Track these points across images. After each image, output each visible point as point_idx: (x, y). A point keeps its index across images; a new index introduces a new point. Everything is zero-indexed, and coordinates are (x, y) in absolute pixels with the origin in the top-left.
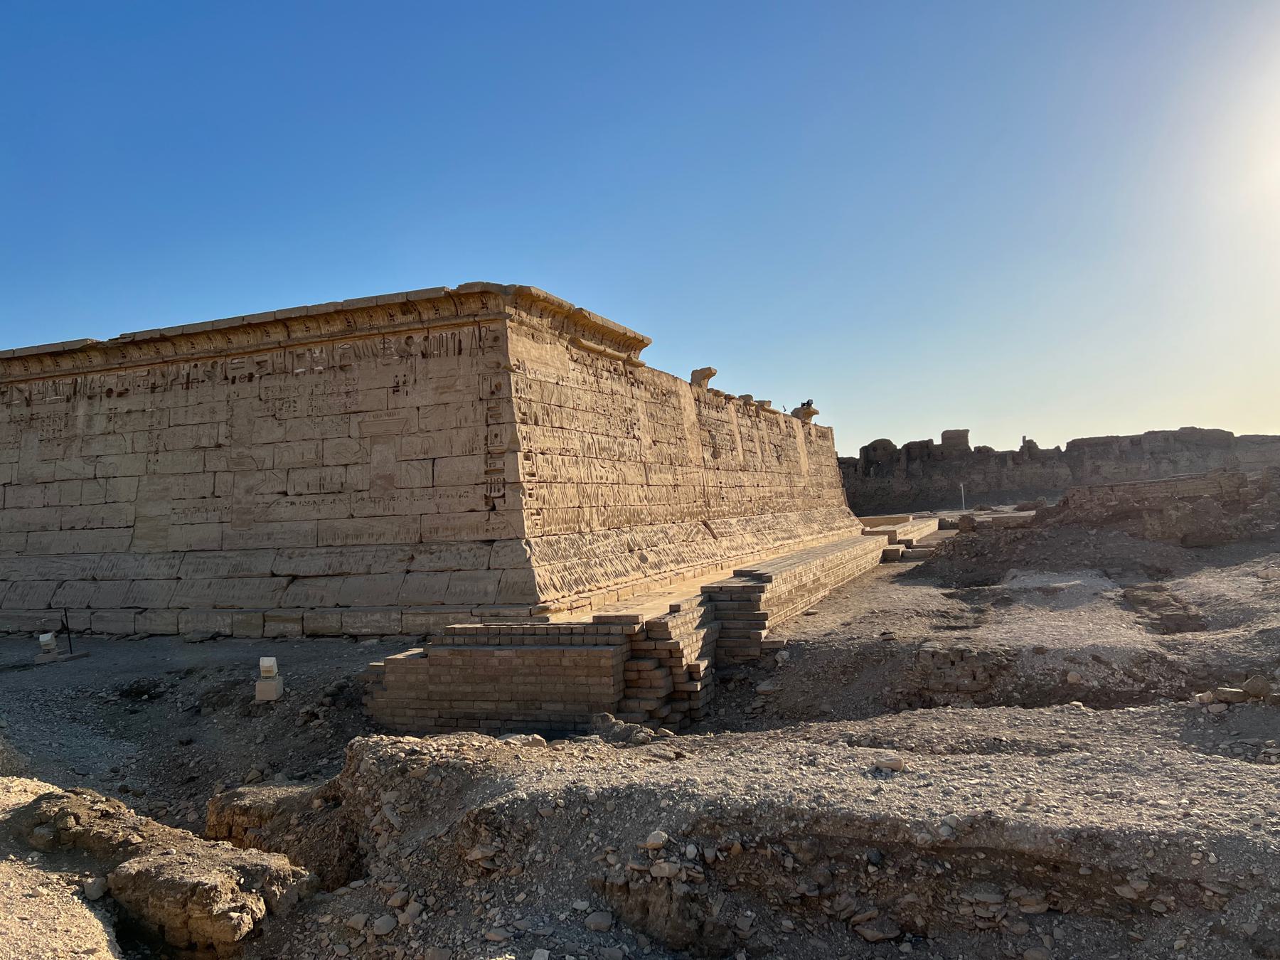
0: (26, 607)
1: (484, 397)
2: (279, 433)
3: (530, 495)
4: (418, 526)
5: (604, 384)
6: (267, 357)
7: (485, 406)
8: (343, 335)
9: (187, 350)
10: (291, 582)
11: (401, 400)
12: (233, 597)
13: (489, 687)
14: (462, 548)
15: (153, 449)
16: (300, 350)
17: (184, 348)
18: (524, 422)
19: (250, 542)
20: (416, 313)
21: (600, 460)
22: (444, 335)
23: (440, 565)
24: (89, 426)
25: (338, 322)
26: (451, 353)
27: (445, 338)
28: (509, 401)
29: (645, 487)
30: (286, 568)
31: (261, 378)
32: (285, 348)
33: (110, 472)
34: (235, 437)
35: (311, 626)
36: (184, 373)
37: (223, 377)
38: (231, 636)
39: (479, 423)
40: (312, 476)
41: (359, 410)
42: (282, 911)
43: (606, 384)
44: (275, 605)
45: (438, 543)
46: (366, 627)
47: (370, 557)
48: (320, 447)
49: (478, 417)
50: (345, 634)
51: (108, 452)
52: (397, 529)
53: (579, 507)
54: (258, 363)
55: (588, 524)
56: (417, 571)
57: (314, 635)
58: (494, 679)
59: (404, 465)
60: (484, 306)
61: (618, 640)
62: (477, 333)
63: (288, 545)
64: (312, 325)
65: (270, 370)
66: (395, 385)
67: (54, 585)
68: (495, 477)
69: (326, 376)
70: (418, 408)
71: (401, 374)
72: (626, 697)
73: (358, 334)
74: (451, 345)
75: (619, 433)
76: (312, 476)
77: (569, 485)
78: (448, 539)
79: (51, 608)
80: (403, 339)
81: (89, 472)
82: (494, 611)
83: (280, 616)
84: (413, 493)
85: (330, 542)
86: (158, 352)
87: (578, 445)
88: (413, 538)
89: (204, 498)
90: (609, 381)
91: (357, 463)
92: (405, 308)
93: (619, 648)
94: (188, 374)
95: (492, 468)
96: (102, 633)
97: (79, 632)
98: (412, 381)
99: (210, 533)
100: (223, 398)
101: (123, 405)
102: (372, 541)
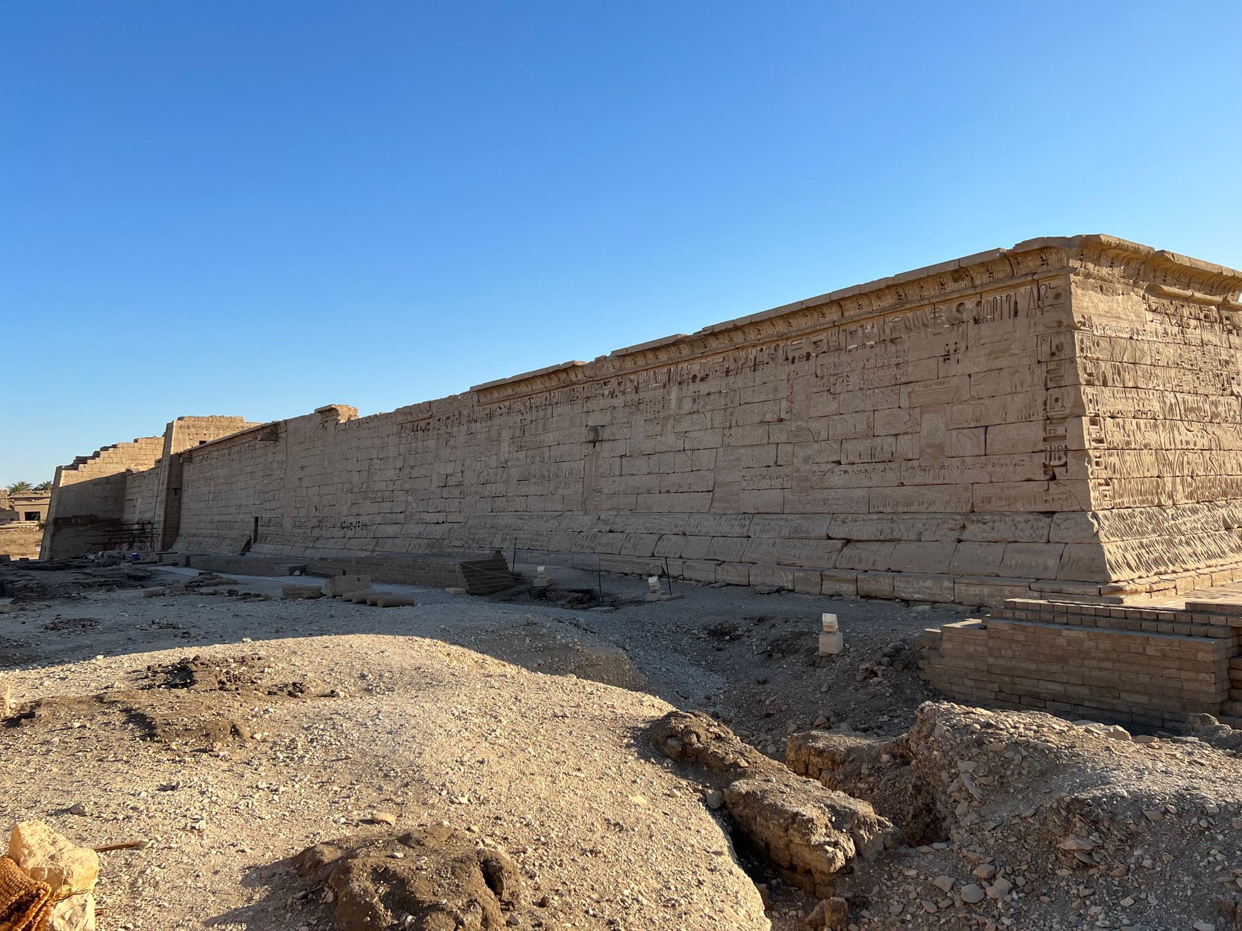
0: (637, 554)
1: (1043, 360)
2: (833, 407)
3: (1097, 464)
4: (969, 494)
5: (1192, 334)
6: (823, 336)
7: (1044, 368)
8: (893, 309)
9: (755, 337)
10: (846, 545)
11: (953, 368)
12: (794, 556)
13: (1055, 668)
14: (1018, 519)
15: (728, 425)
16: (853, 327)
17: (752, 335)
18: (1089, 383)
19: (808, 507)
20: (969, 278)
21: (1186, 423)
22: (998, 298)
23: (994, 535)
24: (680, 407)
25: (889, 297)
26: (1006, 315)
27: (999, 302)
28: (1073, 361)
30: (839, 531)
31: (817, 356)
32: (839, 326)
33: (695, 445)
34: (794, 412)
36: (752, 357)
37: (784, 358)
38: (794, 590)
39: (1037, 388)
41: (909, 380)
42: (870, 854)
43: (1194, 334)
44: (831, 566)
45: (990, 513)
47: (920, 525)
48: (871, 419)
49: (1036, 381)
50: (897, 598)
51: (694, 428)
52: (948, 498)
53: (1158, 477)
55: (1170, 496)
56: (969, 541)
57: (867, 597)
58: (1062, 660)
59: (955, 433)
60: (1044, 262)
61: (1221, 632)
62: (1035, 293)
63: (842, 511)
64: (864, 302)
65: (825, 349)
66: (946, 353)
67: (656, 537)
68: (1055, 444)
69: (877, 349)
70: (970, 375)
71: (951, 342)
72: (1231, 699)
73: (908, 306)
74: (1006, 307)
75: (1211, 390)
76: (862, 446)
77: (1145, 451)
78: (1002, 509)
79: (654, 556)
80: (954, 306)
81: (680, 445)
82: (1056, 587)
84: (963, 461)
85: (881, 509)
86: (731, 340)
87: (1157, 406)
88: (964, 507)
89: (769, 466)
90: (1198, 331)
91: (907, 433)
92: (956, 276)
93: (1222, 643)
94: (756, 357)
95: (1052, 435)
96: (690, 580)
97: (675, 577)
98: (963, 348)
99: (770, 498)
100: (784, 377)
101: (704, 388)
102: (922, 509)
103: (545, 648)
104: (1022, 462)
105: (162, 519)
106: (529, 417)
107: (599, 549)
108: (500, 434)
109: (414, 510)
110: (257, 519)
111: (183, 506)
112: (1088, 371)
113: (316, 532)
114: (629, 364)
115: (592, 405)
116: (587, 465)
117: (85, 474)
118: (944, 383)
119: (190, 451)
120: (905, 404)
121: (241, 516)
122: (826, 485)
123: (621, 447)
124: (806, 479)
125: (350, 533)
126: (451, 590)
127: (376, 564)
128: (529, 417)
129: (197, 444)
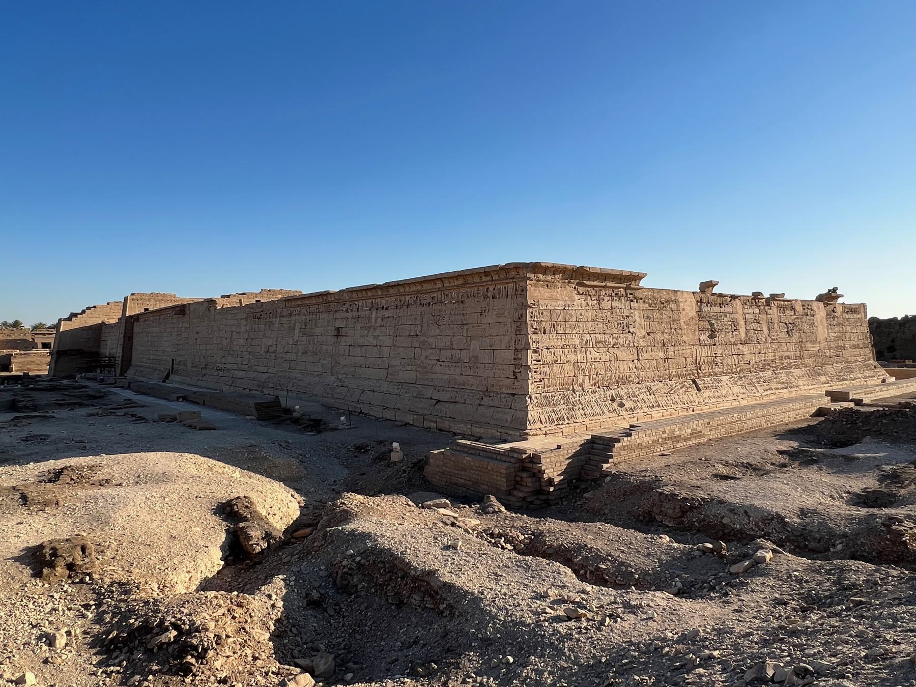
3: (535, 372)
5: (605, 304)
8: (463, 285)
10: (437, 403)
14: (503, 396)
15: (395, 335)
18: (534, 333)
21: (595, 349)
23: (491, 403)
24: (376, 322)
28: (526, 323)
29: (636, 362)
30: (436, 396)
35: (441, 425)
40: (448, 353)
43: (606, 304)
45: (494, 392)
53: (574, 376)
54: (432, 298)
55: (581, 385)
57: (441, 430)
58: (464, 469)
60: (518, 273)
61: (513, 460)
67: (361, 391)
71: (483, 307)
72: (515, 489)
75: (615, 331)
76: (448, 353)
77: (567, 364)
82: (506, 431)
85: (453, 386)
87: (577, 342)
90: (610, 302)
98: (487, 311)
101: (387, 313)
103: (254, 458)
106: (308, 317)
107: (335, 396)
108: (295, 325)
110: (173, 360)
111: (134, 348)
112: (534, 327)
113: (204, 371)
114: (355, 295)
115: (338, 315)
116: (334, 348)
117: (76, 324)
118: (480, 326)
119: (138, 315)
120: (465, 335)
121: (165, 357)
122: (433, 371)
123: (350, 341)
124: (426, 367)
125: (221, 373)
126: (248, 417)
128: (308, 318)
129: (143, 311)
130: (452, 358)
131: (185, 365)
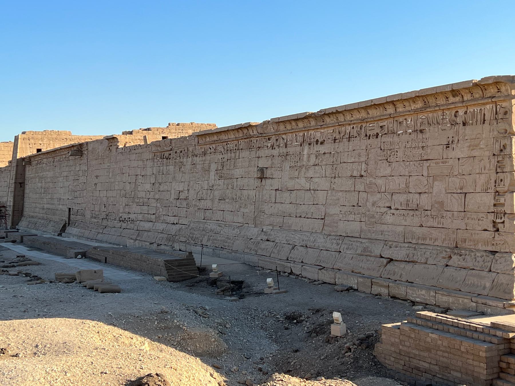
0: (279, 258)
1: (496, 154)
2: (388, 171)
4: (455, 236)
6: (385, 123)
7: (496, 160)
9: (350, 118)
10: (389, 262)
11: (451, 154)
12: (361, 267)
13: (426, 354)
14: (478, 254)
15: (333, 175)
16: (401, 119)
17: (348, 117)
19: (373, 235)
20: (460, 96)
23: (463, 264)
24: (309, 161)
26: (479, 122)
27: (476, 113)
30: (387, 254)
31: (382, 136)
32: (394, 118)
33: (316, 187)
34: (369, 171)
36: (348, 131)
37: (365, 135)
38: (357, 290)
39: (492, 172)
40: (403, 198)
41: (428, 158)
44: (378, 276)
45: (465, 249)
46: (418, 298)
47: (429, 253)
48: (408, 181)
49: (492, 166)
50: (409, 300)
51: (316, 176)
52: (444, 237)
54: (381, 127)
56: (451, 266)
57: (394, 297)
58: (429, 350)
59: (449, 195)
60: (499, 91)
62: (494, 109)
63: (390, 239)
64: (407, 104)
65: (386, 132)
66: (447, 143)
67: (291, 247)
68: (499, 209)
69: (413, 136)
70: (459, 159)
71: (450, 137)
72: (499, 378)
73: (428, 110)
74: (479, 117)
76: (403, 198)
78: (471, 247)
79: (288, 260)
80: (453, 112)
81: (307, 186)
82: (484, 301)
83: (378, 283)
84: (453, 214)
85: (410, 240)
86: (337, 119)
88: (452, 244)
89: (354, 206)
91: (425, 192)
92: (454, 93)
93: (494, 347)
94: (350, 132)
95: (498, 202)
96: (305, 278)
97: (297, 275)
98: (456, 141)
99: (354, 227)
100: (364, 148)
101: (322, 149)
102: (431, 243)
103: (166, 328)
104: (482, 219)
105: (12, 204)
106: (226, 156)
107: (260, 252)
108: (210, 166)
109: (160, 214)
110: (70, 209)
111: (26, 195)
113: (105, 223)
114: (282, 127)
115: (261, 153)
116: (257, 193)
118: (446, 162)
119: (30, 157)
120: (425, 174)
121: (61, 206)
122: (383, 222)
123: (276, 184)
124: (373, 217)
125: (124, 225)
126: (157, 278)
127: (122, 256)
128: (226, 156)
129: (35, 152)
130: (407, 205)
131: (83, 215)
